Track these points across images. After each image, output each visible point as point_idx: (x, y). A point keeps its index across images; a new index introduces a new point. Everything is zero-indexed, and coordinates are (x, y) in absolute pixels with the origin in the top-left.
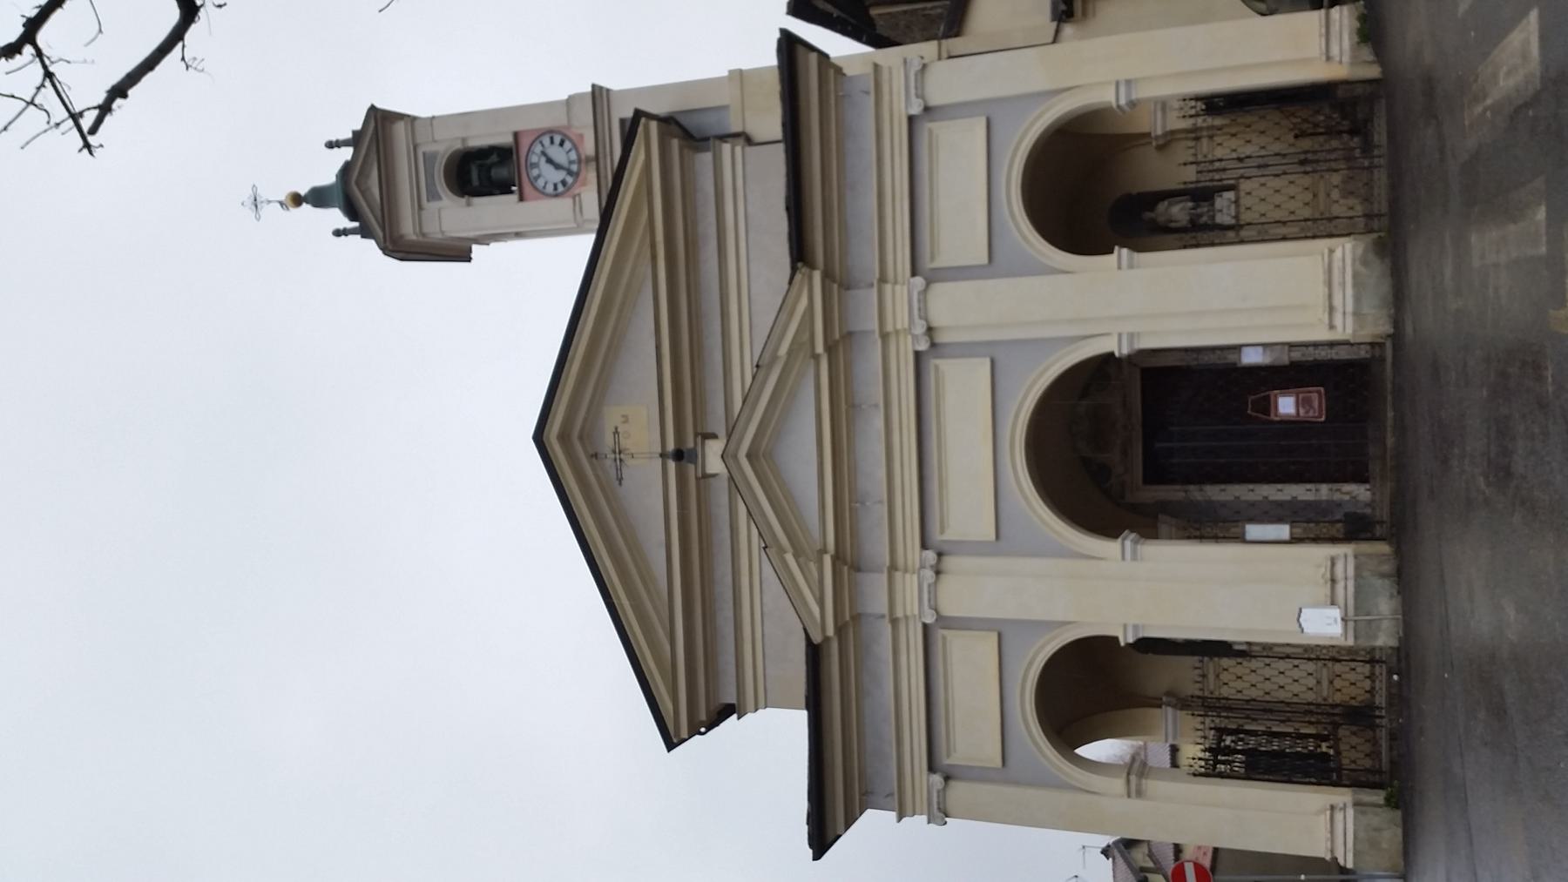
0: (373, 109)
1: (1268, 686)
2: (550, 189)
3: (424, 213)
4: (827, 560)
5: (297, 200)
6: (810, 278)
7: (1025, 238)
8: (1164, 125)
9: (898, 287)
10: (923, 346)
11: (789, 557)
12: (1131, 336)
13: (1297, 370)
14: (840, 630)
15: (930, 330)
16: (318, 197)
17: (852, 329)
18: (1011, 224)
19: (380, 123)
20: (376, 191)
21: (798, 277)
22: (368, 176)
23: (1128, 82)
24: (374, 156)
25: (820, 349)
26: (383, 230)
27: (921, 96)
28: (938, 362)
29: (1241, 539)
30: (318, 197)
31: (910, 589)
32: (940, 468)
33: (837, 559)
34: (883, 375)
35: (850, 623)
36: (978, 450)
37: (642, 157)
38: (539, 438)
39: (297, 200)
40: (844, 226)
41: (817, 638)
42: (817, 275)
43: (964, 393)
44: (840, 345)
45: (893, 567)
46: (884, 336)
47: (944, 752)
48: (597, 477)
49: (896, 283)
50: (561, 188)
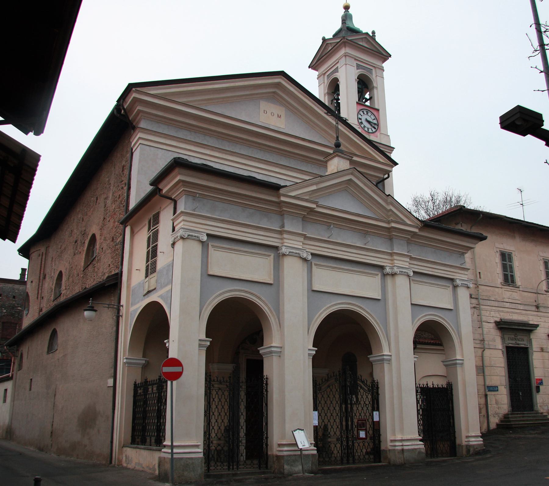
0: (390, 56)
1: (223, 414)
2: (360, 116)
3: (353, 60)
4: (314, 206)
5: (347, 8)
6: (417, 227)
7: (419, 319)
8: (375, 361)
9: (301, 244)
10: (388, 270)
11: (314, 188)
12: (390, 360)
13: (376, 430)
14: (280, 204)
15: (393, 275)
16: (346, 18)
17: (394, 240)
18: (423, 315)
19: (384, 56)
20: (361, 43)
21: (419, 223)
22: (366, 43)
23: (462, 364)
24: (333, 45)
25: (393, 225)
26: (350, 40)
27: (291, 255)
28: (272, 255)
29: (378, 422)
30: (346, 18)
31: (401, 263)
32: (438, 285)
33: (311, 210)
34: (375, 251)
35: (281, 210)
36: (351, 287)
37: (381, 161)
38: (282, 74)
39: (347, 8)
40: (424, 245)
41: (282, 191)
42: (416, 230)
43: (364, 285)
44: (389, 234)
45: (305, 237)
46: (391, 254)
47: (216, 244)
48: (257, 94)
49: (410, 264)
50: (360, 121)
